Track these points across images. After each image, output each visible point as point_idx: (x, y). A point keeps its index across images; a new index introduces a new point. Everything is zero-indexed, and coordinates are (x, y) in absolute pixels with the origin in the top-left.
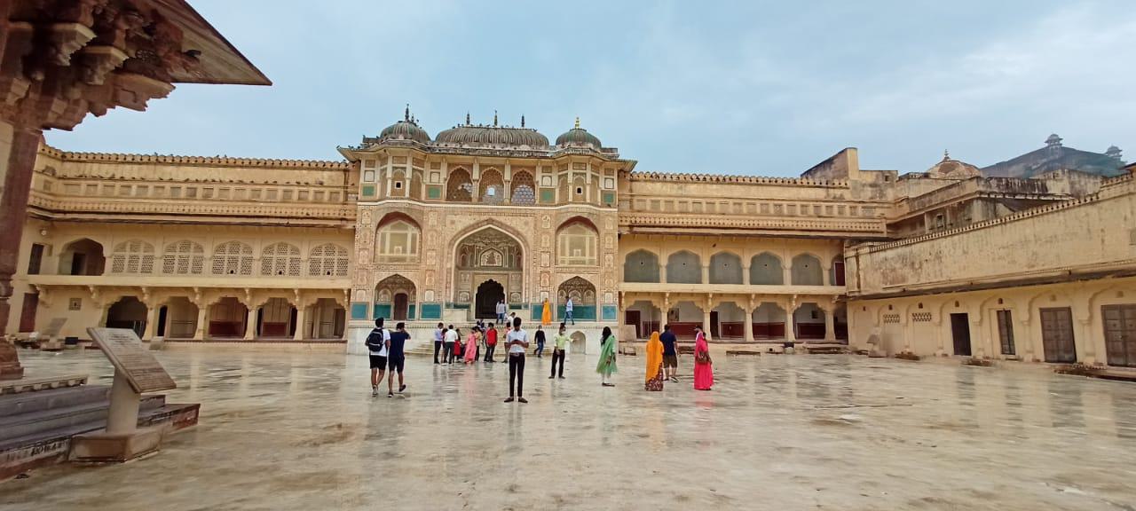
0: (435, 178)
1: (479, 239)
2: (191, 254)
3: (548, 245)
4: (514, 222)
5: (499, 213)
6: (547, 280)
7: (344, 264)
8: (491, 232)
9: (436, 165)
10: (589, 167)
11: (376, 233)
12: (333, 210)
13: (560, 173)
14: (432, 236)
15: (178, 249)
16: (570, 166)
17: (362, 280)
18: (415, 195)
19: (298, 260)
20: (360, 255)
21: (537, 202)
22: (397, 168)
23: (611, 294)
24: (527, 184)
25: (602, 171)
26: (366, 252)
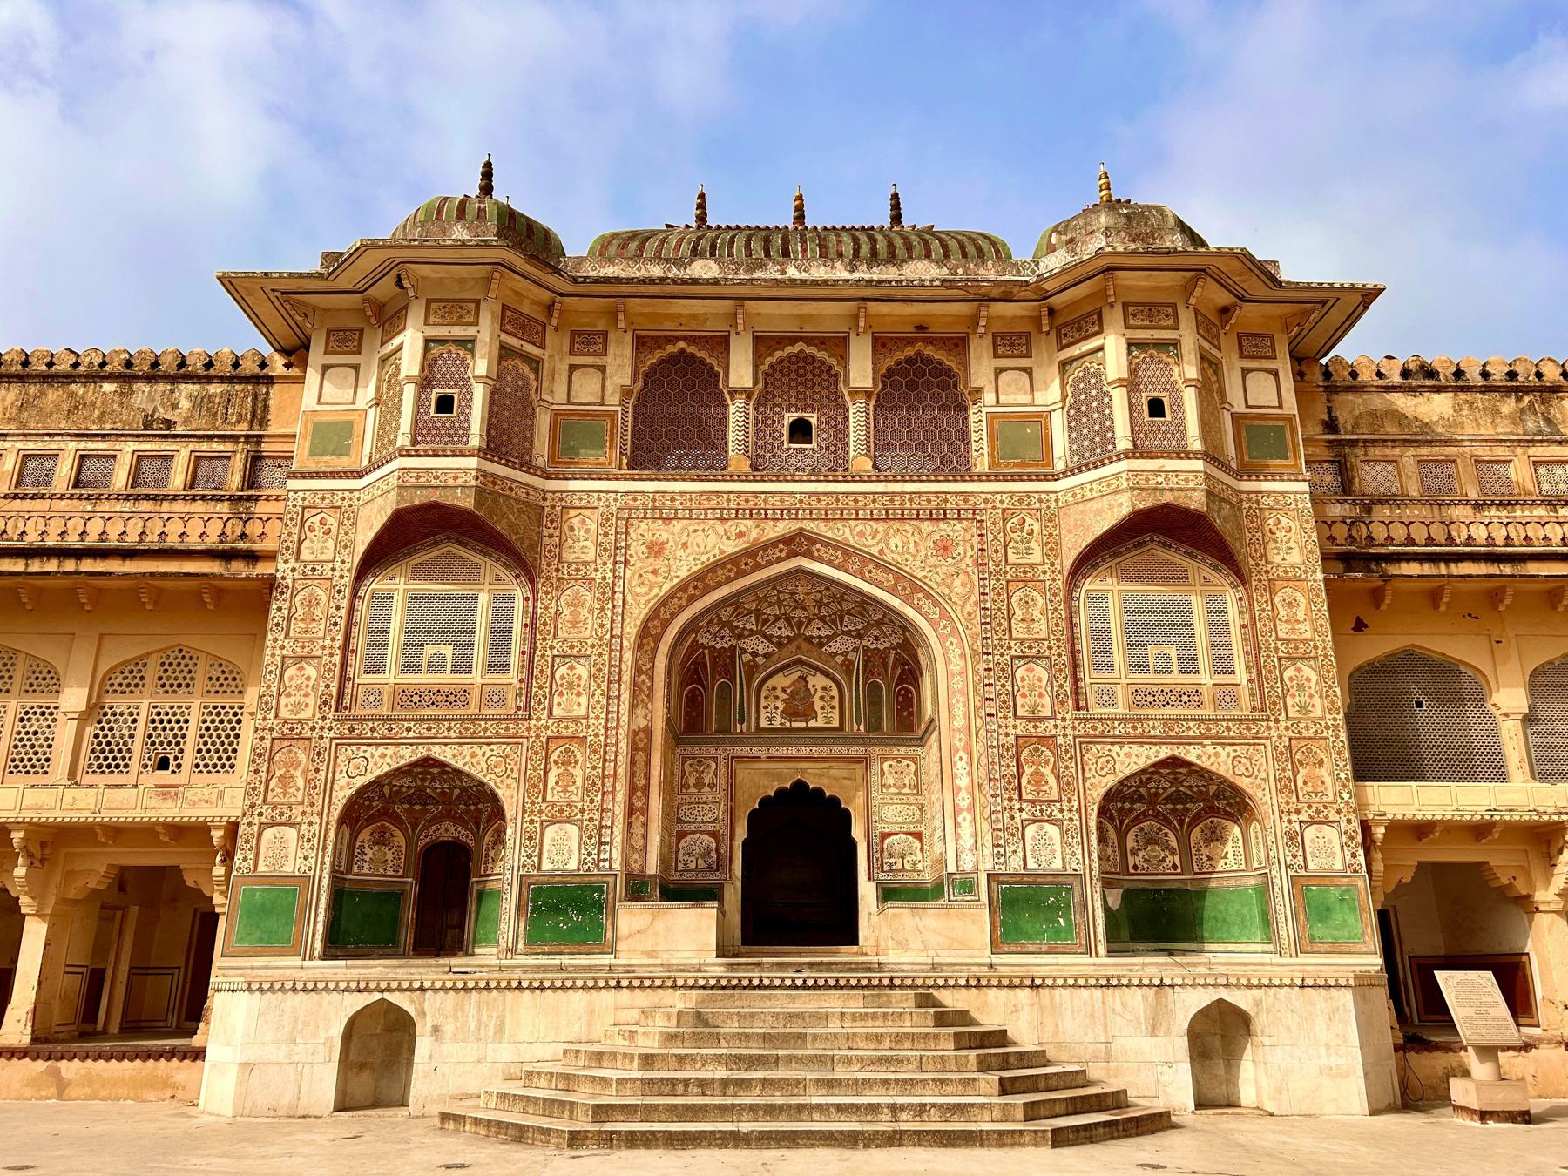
0: (587, 388)
1: (750, 623)
3: (1041, 629)
5: (838, 511)
6: (1047, 771)
8: (802, 591)
9: (588, 342)
10: (1186, 319)
11: (355, 594)
12: (202, 525)
16: (1114, 318)
17: (286, 780)
20: (289, 678)
21: (982, 464)
22: (441, 341)
23: (1331, 833)
24: (935, 399)
26: (311, 671)
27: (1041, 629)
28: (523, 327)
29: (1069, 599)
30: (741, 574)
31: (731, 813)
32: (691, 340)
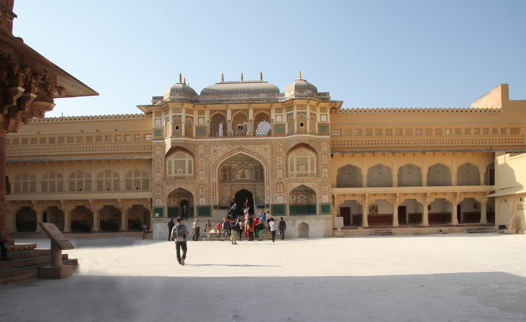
2: (56, 180)
3: (281, 163)
4: (257, 148)
7: (146, 182)
8: (242, 156)
9: (201, 112)
11: (165, 160)
13: (289, 113)
14: (202, 161)
15: (49, 177)
17: (158, 192)
18: (188, 134)
19: (118, 181)
23: (327, 196)
25: (318, 109)
26: (160, 174)
27: (281, 163)
28: (189, 111)
29: (287, 158)
30: (230, 155)
31: (232, 194)
32: (220, 111)
